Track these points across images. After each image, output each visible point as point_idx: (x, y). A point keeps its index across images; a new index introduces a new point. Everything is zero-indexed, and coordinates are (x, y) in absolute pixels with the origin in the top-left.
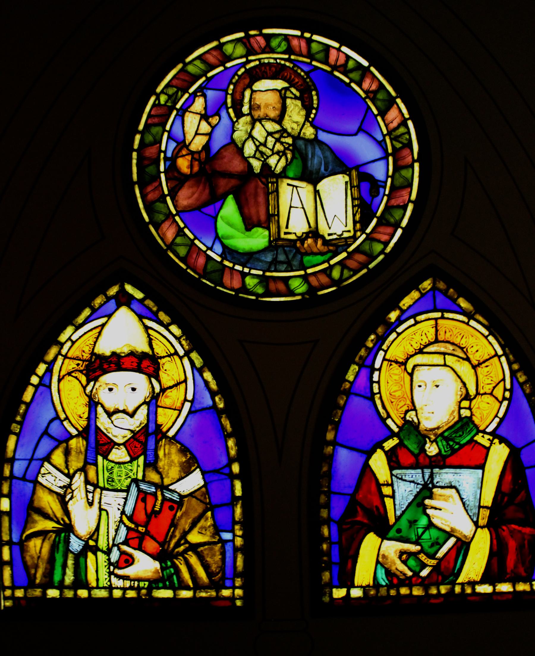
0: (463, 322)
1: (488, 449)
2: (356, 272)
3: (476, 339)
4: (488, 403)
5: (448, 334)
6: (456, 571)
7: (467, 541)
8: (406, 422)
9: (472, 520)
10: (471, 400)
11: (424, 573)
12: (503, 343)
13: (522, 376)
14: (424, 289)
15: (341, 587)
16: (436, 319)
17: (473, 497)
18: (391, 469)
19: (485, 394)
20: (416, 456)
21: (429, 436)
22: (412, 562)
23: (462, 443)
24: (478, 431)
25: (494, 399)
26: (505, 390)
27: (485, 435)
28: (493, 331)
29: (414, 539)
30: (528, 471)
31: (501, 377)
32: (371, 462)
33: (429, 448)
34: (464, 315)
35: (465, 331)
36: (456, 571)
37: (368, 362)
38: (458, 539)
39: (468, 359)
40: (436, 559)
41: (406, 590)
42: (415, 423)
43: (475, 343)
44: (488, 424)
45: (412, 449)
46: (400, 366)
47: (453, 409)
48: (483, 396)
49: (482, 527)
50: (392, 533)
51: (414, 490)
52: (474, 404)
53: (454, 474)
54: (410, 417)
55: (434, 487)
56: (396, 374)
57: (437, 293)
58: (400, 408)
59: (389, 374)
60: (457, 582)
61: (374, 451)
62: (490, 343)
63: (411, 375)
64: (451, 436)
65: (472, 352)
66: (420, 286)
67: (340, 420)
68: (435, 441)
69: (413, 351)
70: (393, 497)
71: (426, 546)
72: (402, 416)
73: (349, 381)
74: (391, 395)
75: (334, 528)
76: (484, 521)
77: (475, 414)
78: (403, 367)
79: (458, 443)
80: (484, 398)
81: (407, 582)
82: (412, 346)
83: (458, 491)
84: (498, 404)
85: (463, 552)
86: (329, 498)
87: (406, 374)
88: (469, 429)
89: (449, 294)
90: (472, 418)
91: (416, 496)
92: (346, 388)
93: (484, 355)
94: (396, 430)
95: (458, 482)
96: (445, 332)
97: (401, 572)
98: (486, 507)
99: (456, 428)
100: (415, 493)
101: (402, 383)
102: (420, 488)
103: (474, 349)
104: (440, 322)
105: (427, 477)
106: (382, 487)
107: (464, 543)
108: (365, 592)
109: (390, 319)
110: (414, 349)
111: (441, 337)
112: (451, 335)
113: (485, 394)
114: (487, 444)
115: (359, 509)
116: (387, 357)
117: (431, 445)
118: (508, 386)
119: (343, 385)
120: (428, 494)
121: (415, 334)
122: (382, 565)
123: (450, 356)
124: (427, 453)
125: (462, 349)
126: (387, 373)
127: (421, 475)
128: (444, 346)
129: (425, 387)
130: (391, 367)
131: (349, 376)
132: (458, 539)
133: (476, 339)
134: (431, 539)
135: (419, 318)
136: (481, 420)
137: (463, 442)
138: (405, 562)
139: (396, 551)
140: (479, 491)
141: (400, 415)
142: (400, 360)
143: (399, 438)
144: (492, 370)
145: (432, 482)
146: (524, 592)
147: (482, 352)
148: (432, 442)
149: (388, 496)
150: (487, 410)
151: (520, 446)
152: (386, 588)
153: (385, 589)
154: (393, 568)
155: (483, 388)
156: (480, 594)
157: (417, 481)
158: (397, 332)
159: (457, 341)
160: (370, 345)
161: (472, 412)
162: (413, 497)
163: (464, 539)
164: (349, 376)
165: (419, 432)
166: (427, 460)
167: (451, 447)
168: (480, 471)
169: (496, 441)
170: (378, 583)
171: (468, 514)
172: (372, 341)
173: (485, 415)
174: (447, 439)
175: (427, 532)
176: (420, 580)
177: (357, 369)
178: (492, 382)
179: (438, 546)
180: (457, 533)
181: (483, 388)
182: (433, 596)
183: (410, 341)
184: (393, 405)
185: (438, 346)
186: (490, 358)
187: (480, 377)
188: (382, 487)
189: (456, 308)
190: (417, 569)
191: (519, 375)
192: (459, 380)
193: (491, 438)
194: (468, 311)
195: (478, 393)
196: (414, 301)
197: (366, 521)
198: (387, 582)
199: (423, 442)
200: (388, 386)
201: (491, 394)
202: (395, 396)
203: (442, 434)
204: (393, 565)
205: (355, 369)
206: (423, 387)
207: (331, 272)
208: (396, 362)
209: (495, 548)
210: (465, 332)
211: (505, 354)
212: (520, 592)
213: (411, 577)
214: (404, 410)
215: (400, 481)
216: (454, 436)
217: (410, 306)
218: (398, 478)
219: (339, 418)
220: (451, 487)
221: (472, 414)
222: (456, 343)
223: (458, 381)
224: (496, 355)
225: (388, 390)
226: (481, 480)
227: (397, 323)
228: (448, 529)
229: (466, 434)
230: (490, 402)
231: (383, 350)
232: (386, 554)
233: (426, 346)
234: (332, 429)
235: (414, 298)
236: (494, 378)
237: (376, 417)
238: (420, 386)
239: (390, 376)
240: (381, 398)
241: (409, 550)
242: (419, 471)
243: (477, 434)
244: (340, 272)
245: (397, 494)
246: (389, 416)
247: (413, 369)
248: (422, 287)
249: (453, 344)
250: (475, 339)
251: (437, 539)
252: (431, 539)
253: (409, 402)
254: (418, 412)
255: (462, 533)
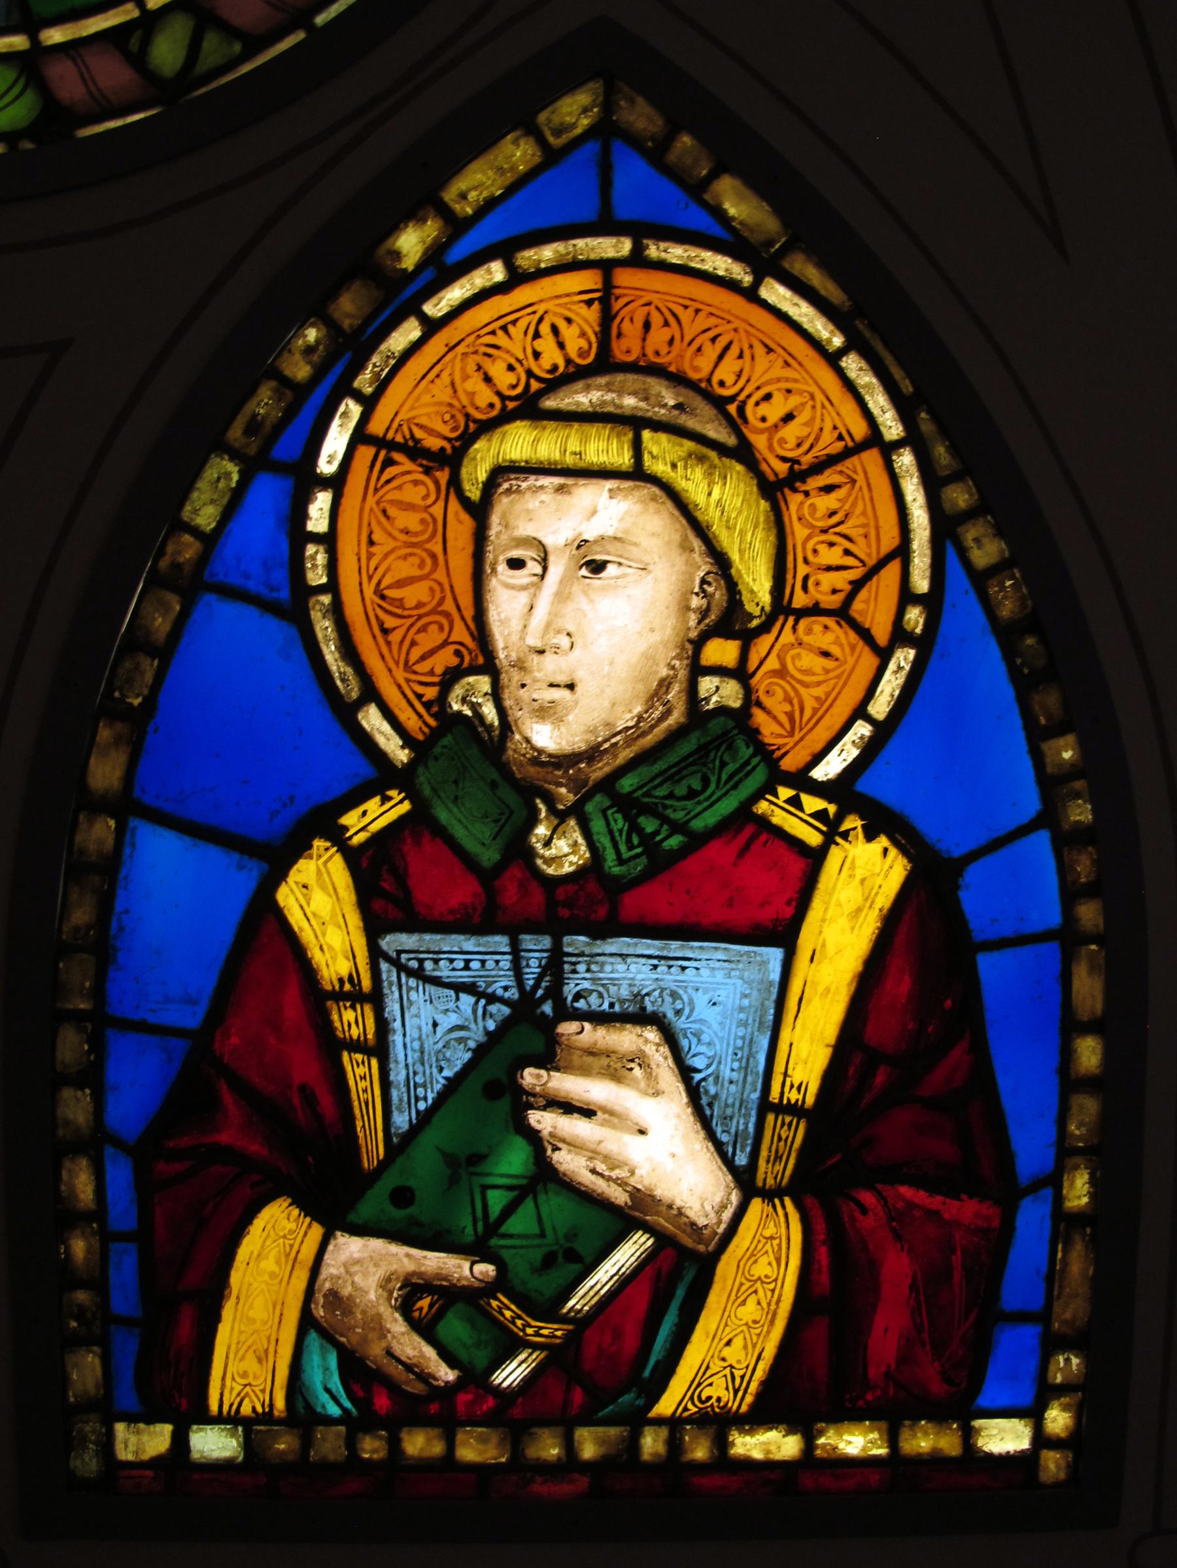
0: (728, 284)
1: (815, 858)
2: (254, 45)
3: (787, 364)
4: (826, 654)
5: (658, 336)
6: (647, 1373)
7: (701, 1248)
8: (448, 722)
9: (728, 1162)
10: (747, 638)
11: (511, 1374)
12: (907, 387)
13: (985, 541)
14: (558, 132)
15: (151, 1418)
16: (607, 267)
17: (736, 1065)
18: (374, 929)
19: (815, 610)
20: (487, 877)
21: (552, 787)
22: (454, 1328)
23: (698, 824)
24: (777, 777)
25: (853, 636)
26: (906, 596)
27: (807, 800)
28: (867, 334)
29: (469, 1235)
30: (984, 962)
31: (890, 539)
32: (287, 896)
33: (548, 843)
34: (737, 256)
35: (737, 323)
36: (647, 1373)
37: (287, 448)
38: (663, 1240)
39: (744, 453)
40: (564, 1319)
41: (428, 1441)
42: (489, 728)
43: (779, 380)
44: (819, 746)
45: (470, 845)
46: (427, 471)
47: (664, 672)
48: (803, 624)
49: (769, 1195)
50: (375, 1202)
51: (473, 1026)
52: (763, 653)
53: (655, 962)
54: (464, 700)
55: (566, 1013)
56: (409, 507)
57: (618, 148)
58: (423, 658)
59: (378, 503)
60: (653, 1413)
61: (297, 848)
62: (850, 386)
63: (480, 511)
64: (645, 795)
65: (764, 419)
66: (542, 117)
67: (150, 703)
68: (577, 811)
69: (492, 406)
70: (379, 1049)
71: (521, 1265)
72: (431, 693)
73: (196, 532)
74: (383, 597)
75: (120, 1171)
76: (779, 1167)
77: (767, 701)
78: (443, 476)
79: (676, 828)
80: (809, 631)
81: (434, 1408)
82: (488, 379)
83: (670, 1038)
84: (869, 661)
85: (680, 1293)
86: (97, 1044)
87: (454, 505)
88: (731, 768)
89: (672, 157)
90: (750, 716)
91: (480, 1052)
92: (181, 560)
93: (817, 439)
94: (399, 753)
95: (674, 995)
96: (647, 326)
97: (409, 1368)
98: (795, 1110)
99: (673, 757)
100: (476, 1036)
101: (437, 548)
102: (499, 1018)
103: (774, 411)
104: (625, 278)
105: (532, 969)
106: (329, 1003)
107: (685, 1254)
108: (248, 1445)
109: (397, 255)
110: (499, 394)
111: (627, 347)
112: (671, 342)
113: (815, 610)
114: (813, 838)
115: (227, 1097)
116: (377, 426)
117: (554, 831)
118: (921, 583)
119: (170, 548)
120: (537, 1044)
121: (504, 328)
122: (328, 1336)
123: (663, 437)
124: (539, 862)
125: (719, 403)
126: (371, 500)
127: (506, 962)
128: (638, 385)
129: (538, 569)
130: (391, 471)
131: (198, 504)
132: (663, 1240)
133: (787, 364)
134: (542, 1235)
135: (528, 258)
136: (787, 726)
137: (709, 819)
138: (425, 1329)
139: (388, 1280)
140: (764, 1042)
141: (420, 689)
142: (433, 443)
143: (412, 794)
144: (854, 505)
145: (555, 992)
146: (935, 1460)
147: (809, 423)
148: (560, 817)
149: (356, 1046)
150: (819, 684)
151: (957, 853)
152: (342, 1429)
153: (338, 1434)
154: (376, 1350)
155: (805, 588)
156: (748, 1464)
157: (489, 984)
158: (424, 319)
159: (700, 367)
160: (301, 371)
161: (748, 691)
162: (468, 1055)
163: (688, 1242)
164: (198, 504)
165: (504, 769)
166: (538, 896)
167: (649, 843)
168: (774, 956)
169: (853, 822)
170: (309, 1407)
171: (711, 1135)
172: (309, 350)
173: (809, 704)
174: (629, 806)
175: (529, 1203)
176: (490, 1402)
177: (235, 477)
178: (849, 561)
179: (576, 1268)
180: (658, 1214)
181: (805, 588)
182: (545, 1469)
183: (478, 358)
184: (388, 643)
185: (609, 388)
186: (847, 453)
187: (798, 533)
188: (329, 1003)
189: (702, 221)
190: (481, 1359)
191: (970, 533)
192: (697, 543)
193: (832, 809)
194: (756, 238)
195: (781, 607)
196: (509, 178)
197: (255, 1148)
198: (347, 1404)
199: (521, 814)
200: (370, 556)
201: (842, 614)
202: (400, 603)
203: (607, 784)
204: (372, 1335)
205: (228, 475)
206: (534, 567)
207: (146, 42)
208: (415, 451)
209: (824, 1279)
210: (735, 330)
211: (913, 439)
212: (919, 1461)
213: (450, 1390)
214: (439, 670)
215: (412, 982)
216: (661, 792)
217: (490, 204)
218: (401, 968)
219: (146, 692)
220: (641, 1017)
221: (750, 700)
222: (694, 376)
223: (692, 550)
224: (874, 438)
225: (370, 578)
226: (775, 991)
227: (429, 274)
228: (619, 1197)
229: (717, 786)
230: (835, 650)
231: (358, 397)
232: (346, 1291)
233: (557, 382)
234: (117, 741)
235: (513, 168)
236: (861, 541)
237: (312, 693)
238: (516, 564)
239: (384, 512)
240: (337, 611)
241: (445, 1278)
242: (501, 942)
243: (769, 788)
244: (186, 42)
245: (397, 1039)
246: (370, 693)
247: (490, 486)
248: (549, 120)
249: (678, 380)
250: (780, 363)
251: (572, 1235)
252: (542, 1235)
253: (461, 634)
254: (504, 678)
255: (680, 1213)
